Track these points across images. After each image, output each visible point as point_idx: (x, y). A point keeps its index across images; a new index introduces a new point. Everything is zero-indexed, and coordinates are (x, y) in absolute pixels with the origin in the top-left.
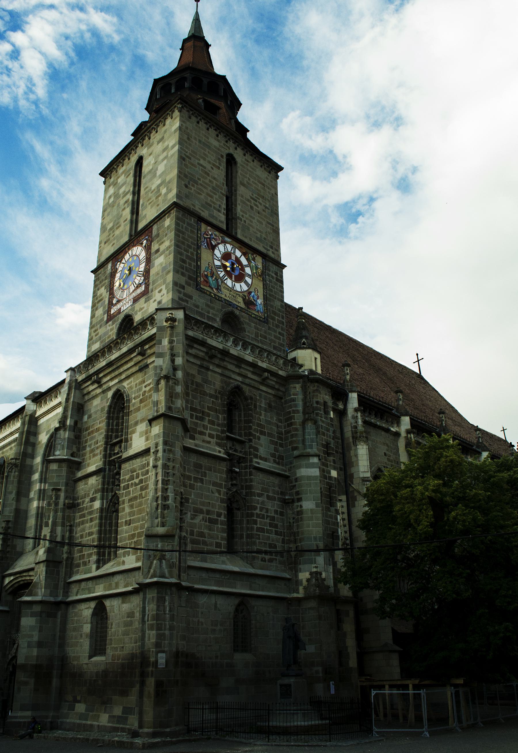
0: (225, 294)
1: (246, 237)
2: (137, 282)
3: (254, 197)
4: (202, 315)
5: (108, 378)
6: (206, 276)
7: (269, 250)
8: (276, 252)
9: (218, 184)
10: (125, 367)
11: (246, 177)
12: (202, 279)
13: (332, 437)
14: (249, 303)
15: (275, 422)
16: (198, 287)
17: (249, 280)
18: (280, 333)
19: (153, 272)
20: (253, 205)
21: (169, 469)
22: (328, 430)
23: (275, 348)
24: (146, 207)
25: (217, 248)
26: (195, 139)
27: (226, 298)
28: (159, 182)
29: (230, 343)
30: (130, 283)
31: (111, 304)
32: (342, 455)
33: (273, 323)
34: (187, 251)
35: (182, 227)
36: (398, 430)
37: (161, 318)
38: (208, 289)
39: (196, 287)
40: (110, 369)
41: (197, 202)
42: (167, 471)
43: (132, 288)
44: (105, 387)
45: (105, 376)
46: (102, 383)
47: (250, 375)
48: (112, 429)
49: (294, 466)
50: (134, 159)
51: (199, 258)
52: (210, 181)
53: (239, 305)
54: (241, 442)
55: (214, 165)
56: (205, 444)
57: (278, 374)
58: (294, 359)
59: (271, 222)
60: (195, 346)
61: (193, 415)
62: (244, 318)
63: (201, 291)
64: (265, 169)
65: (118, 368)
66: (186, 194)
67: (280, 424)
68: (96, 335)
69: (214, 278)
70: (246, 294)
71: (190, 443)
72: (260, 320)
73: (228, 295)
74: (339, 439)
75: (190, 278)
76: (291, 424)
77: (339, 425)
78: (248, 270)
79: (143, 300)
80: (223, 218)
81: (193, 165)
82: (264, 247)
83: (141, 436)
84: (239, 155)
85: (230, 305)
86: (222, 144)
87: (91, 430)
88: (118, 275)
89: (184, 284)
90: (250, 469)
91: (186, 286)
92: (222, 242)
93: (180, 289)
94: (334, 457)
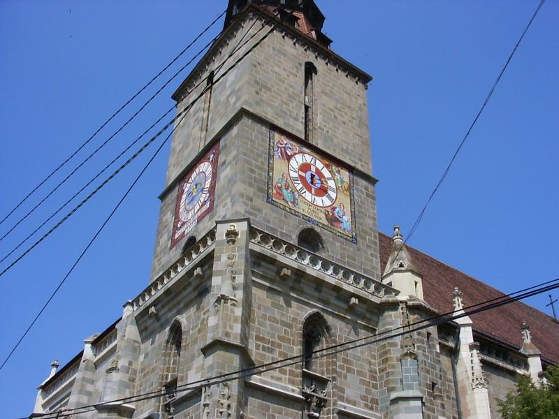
0: (302, 208)
1: (328, 148)
2: (202, 200)
3: (339, 106)
4: (272, 229)
5: (166, 309)
6: (280, 188)
8: (366, 166)
9: (296, 92)
10: (184, 293)
11: (329, 86)
12: (274, 191)
13: (439, 376)
14: (333, 220)
15: (366, 357)
16: (269, 200)
17: (333, 195)
18: (372, 255)
19: (218, 186)
20: (337, 115)
21: (223, 408)
22: (434, 368)
24: (215, 121)
26: (269, 46)
27: (304, 213)
28: (228, 92)
29: (307, 261)
30: (196, 202)
31: (176, 228)
32: (456, 402)
33: (363, 243)
34: (256, 160)
35: (251, 135)
36: (526, 372)
37: (222, 231)
38: (283, 202)
40: (169, 298)
41: (269, 110)
42: (221, 410)
43: (197, 207)
44: (163, 320)
45: (163, 307)
46: (160, 315)
47: (333, 300)
48: (168, 368)
49: (390, 412)
50: (206, 75)
51: (270, 169)
52: (286, 89)
53: (320, 221)
54: (323, 383)
55: (290, 72)
56: (273, 381)
58: (390, 284)
59: (359, 134)
60: (263, 263)
61: (260, 345)
62: (326, 235)
65: (177, 295)
66: (256, 101)
67: (373, 361)
68: (159, 264)
69: (289, 191)
70: (329, 209)
71: (255, 380)
72: (346, 239)
73: (306, 210)
74: (451, 382)
75: (260, 190)
76: (387, 360)
77: (451, 365)
78: (331, 184)
79: (207, 217)
80: (302, 127)
81: (265, 72)
82: (350, 159)
83: (197, 372)
84: (320, 64)
85: (309, 221)
86: (300, 52)
87: (146, 371)
88: (184, 196)
89: (251, 195)
90: (333, 414)
91: (254, 198)
92: (299, 152)
93: (247, 202)
94: (443, 400)
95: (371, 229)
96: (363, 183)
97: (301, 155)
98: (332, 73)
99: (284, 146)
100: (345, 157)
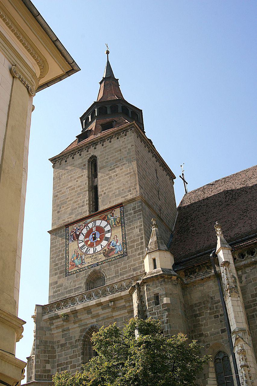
3: (112, 168)
7: (127, 195)
12: (70, 266)
23: (134, 270)
25: (81, 234)
39: (66, 275)
51: (67, 253)
53: (101, 260)
57: (121, 297)
60: (54, 321)
63: (69, 275)
64: (122, 137)
69: (79, 258)
70: (106, 248)
75: (61, 273)
82: (122, 197)
92: (85, 227)
95: (138, 236)
96: (132, 205)
97: (86, 227)
98: (107, 148)
99: (74, 232)
100: (118, 199)
